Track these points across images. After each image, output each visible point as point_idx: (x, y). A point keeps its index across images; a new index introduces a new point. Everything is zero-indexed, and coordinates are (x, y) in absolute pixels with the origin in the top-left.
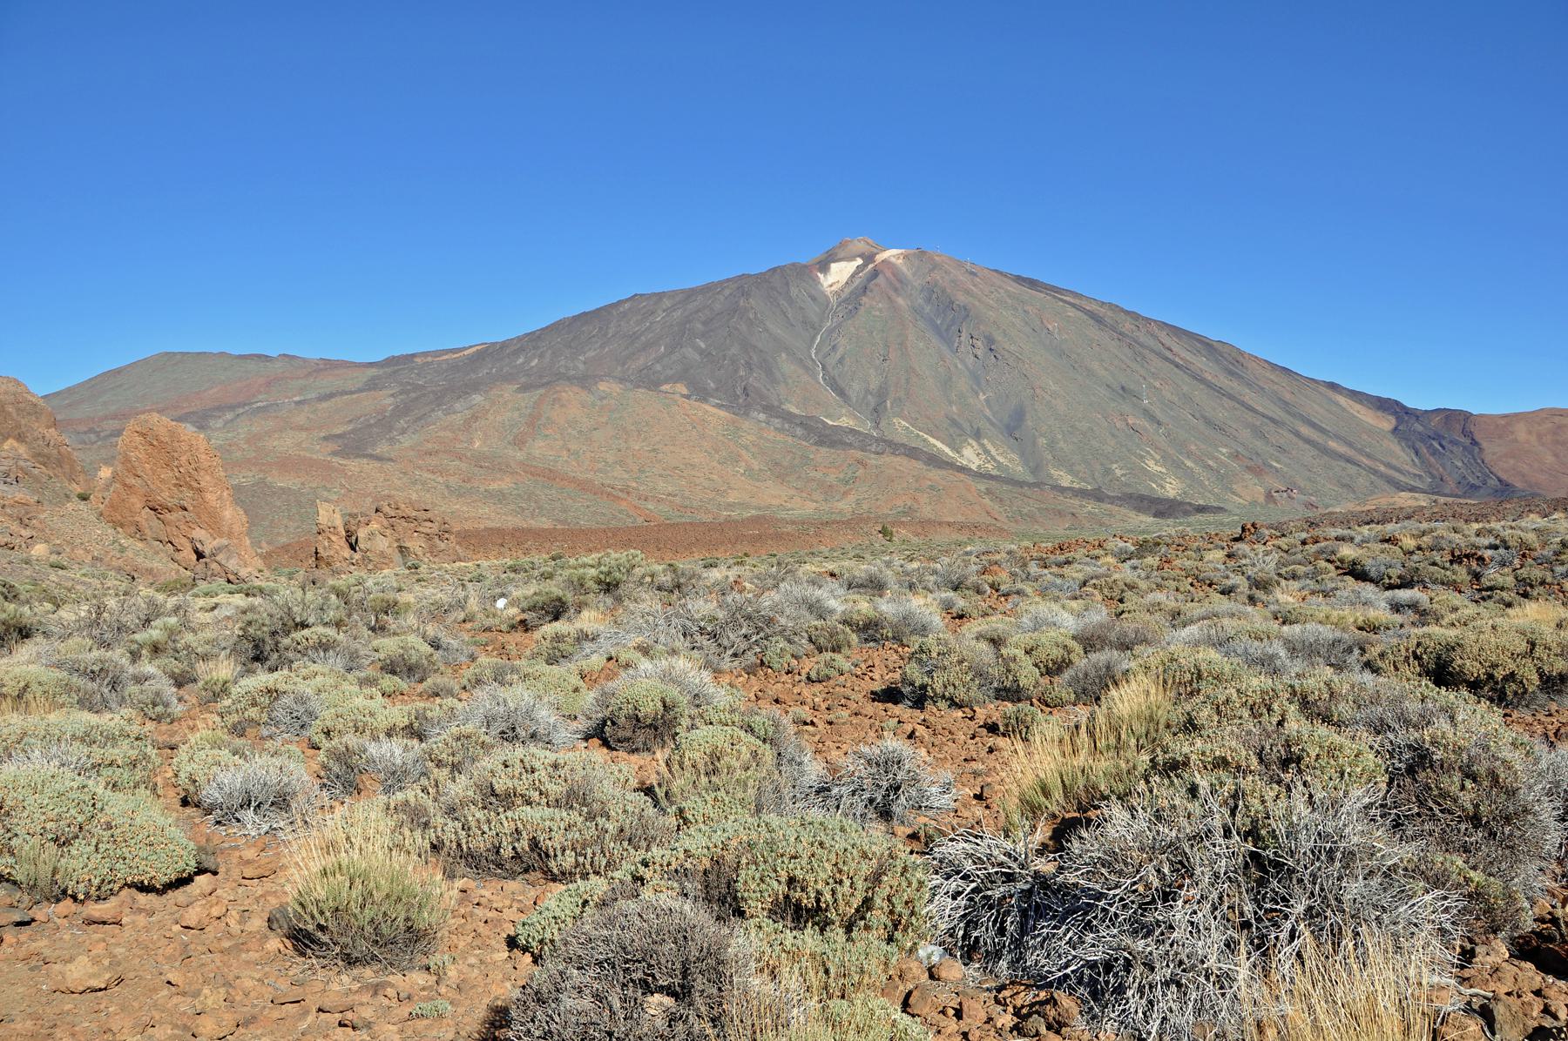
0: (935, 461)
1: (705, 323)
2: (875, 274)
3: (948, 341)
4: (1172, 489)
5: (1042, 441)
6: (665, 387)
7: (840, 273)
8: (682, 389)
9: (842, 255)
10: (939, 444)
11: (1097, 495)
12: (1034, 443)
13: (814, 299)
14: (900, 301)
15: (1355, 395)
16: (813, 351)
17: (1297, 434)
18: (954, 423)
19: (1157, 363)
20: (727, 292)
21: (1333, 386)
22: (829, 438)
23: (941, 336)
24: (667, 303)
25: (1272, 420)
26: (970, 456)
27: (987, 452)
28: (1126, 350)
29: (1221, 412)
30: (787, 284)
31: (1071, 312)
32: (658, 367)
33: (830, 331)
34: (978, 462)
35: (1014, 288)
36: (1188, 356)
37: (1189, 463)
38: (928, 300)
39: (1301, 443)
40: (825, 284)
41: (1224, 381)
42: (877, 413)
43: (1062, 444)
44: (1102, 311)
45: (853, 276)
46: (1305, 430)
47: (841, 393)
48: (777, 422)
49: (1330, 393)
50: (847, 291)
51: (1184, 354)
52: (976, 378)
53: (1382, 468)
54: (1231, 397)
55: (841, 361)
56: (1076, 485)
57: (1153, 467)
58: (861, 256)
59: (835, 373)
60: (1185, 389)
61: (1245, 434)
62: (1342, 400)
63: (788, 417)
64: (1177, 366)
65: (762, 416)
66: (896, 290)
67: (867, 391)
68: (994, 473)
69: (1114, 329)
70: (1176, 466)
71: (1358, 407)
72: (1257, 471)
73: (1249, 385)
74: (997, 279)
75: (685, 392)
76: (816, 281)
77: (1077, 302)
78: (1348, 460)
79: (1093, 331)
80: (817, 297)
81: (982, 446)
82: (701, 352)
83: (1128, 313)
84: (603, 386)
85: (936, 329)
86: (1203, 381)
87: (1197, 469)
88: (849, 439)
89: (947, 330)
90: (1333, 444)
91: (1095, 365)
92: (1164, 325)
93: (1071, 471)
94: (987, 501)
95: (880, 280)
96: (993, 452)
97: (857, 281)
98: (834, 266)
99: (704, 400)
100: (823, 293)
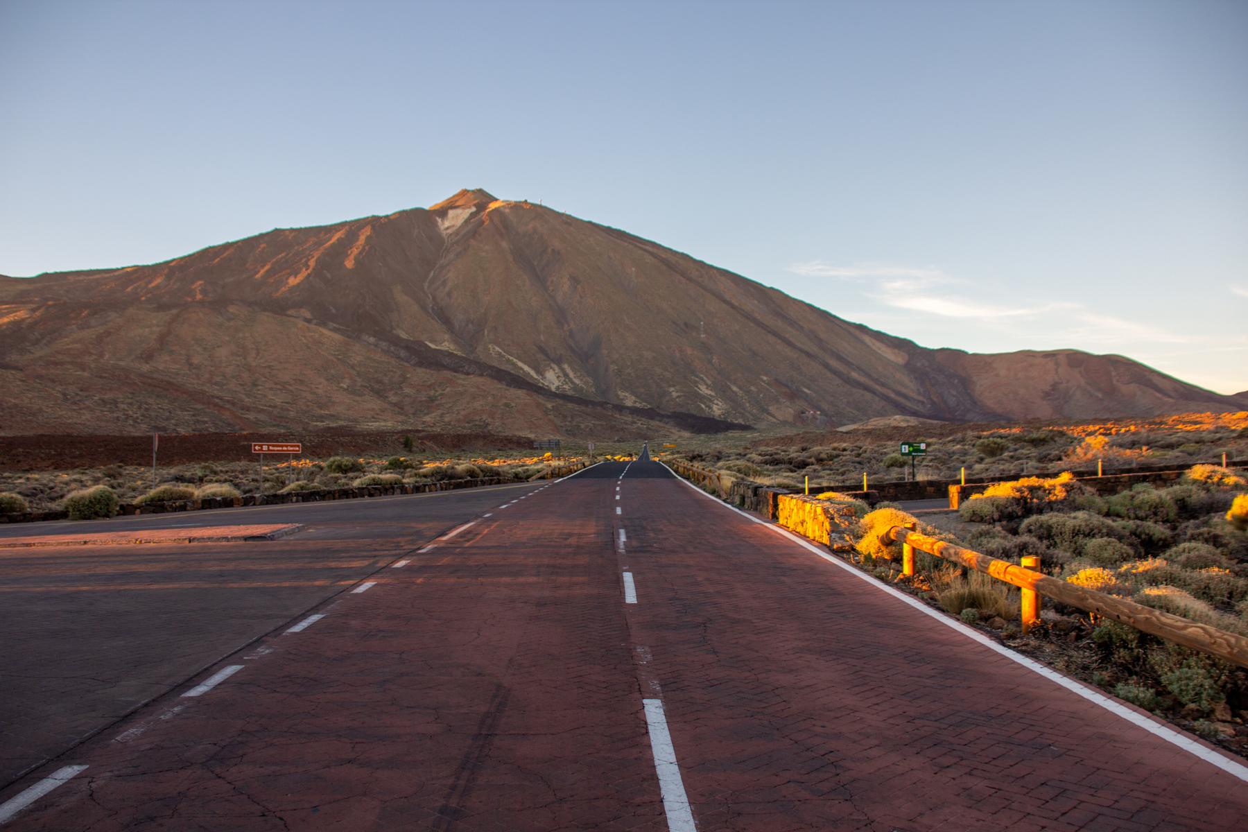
0: (518, 381)
4: (718, 409)
5: (613, 367)
6: (289, 312)
10: (526, 368)
11: (650, 414)
15: (879, 336)
16: (426, 285)
17: (827, 366)
18: (542, 350)
21: (861, 328)
22: (431, 360)
25: (808, 355)
26: (552, 379)
27: (566, 375)
31: (649, 259)
34: (557, 383)
37: (735, 389)
39: (829, 374)
40: (442, 228)
45: (467, 221)
46: (833, 363)
48: (384, 345)
49: (858, 333)
53: (892, 395)
54: (775, 334)
55: (449, 294)
56: (638, 405)
57: (704, 390)
62: (867, 339)
63: (396, 342)
64: (733, 307)
65: (372, 340)
68: (570, 393)
70: (722, 391)
71: (878, 344)
72: (793, 395)
75: (308, 315)
76: (435, 225)
77: (655, 251)
78: (867, 388)
80: (435, 238)
81: (563, 370)
84: (232, 309)
87: (740, 393)
88: (446, 361)
90: (854, 375)
93: (634, 393)
94: (552, 417)
96: (571, 375)
97: (470, 226)
98: (451, 213)
99: (323, 324)
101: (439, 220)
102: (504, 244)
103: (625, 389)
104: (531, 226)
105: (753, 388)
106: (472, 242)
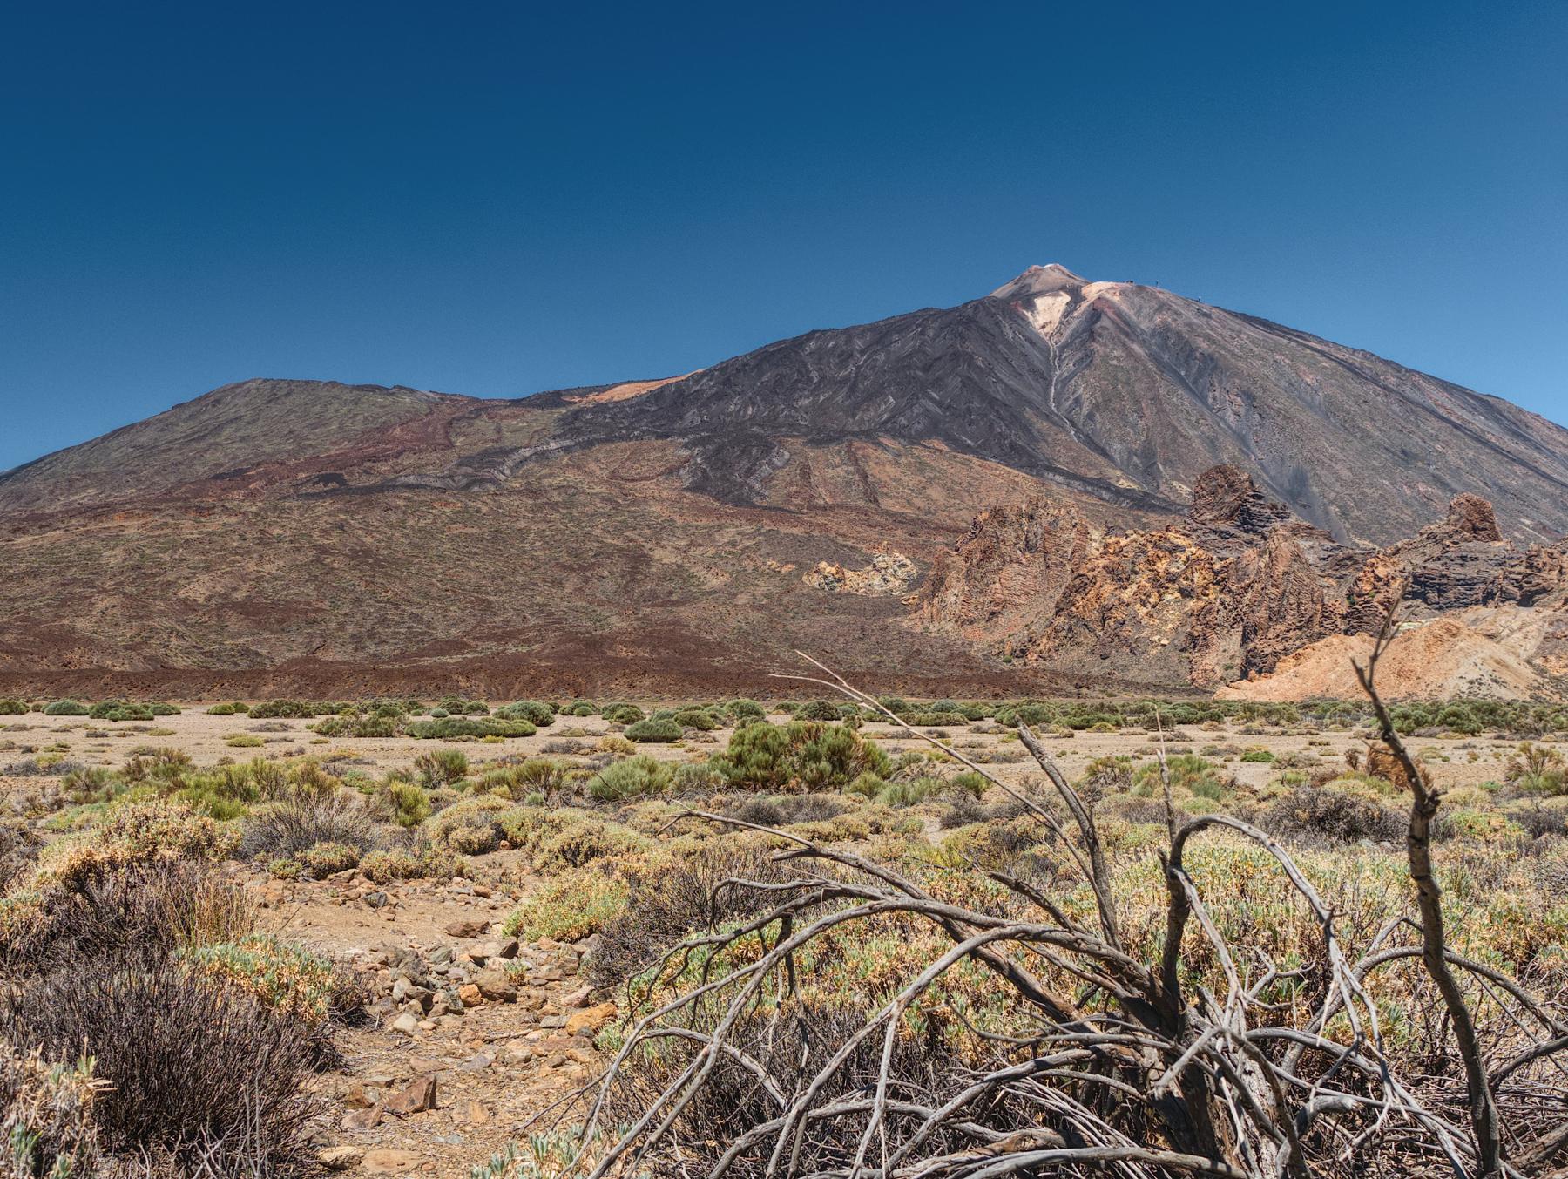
1: (927, 369)
2: (1095, 314)
3: (1203, 399)
5: (1333, 509)
7: (1048, 312)
8: (936, 443)
9: (1036, 287)
12: (1327, 513)
13: (1032, 343)
14: (1136, 348)
16: (1053, 406)
19: (1436, 424)
20: (931, 333)
23: (1191, 390)
24: (859, 344)
28: (1396, 407)
29: (1516, 478)
30: (997, 324)
32: (904, 421)
33: (1065, 382)
35: (1251, 332)
36: (1466, 415)
38: (1164, 347)
40: (1037, 325)
41: (1509, 443)
42: (1149, 472)
43: (1356, 513)
44: (1357, 360)
45: (1066, 314)
47: (1104, 453)
50: (1067, 333)
51: (1461, 412)
52: (1241, 439)
54: (1522, 463)
55: (1090, 416)
58: (1063, 288)
59: (1088, 429)
60: (1471, 454)
61: (1545, 504)
64: (1456, 426)
66: (1127, 335)
67: (1131, 452)
69: (1375, 382)
73: (1538, 448)
74: (1236, 324)
76: (1024, 319)
77: (1326, 349)
79: (1355, 386)
82: (939, 404)
83: (1387, 363)
85: (1182, 382)
86: (1486, 443)
89: (1195, 382)
91: (1368, 425)
92: (1430, 379)
95: (1104, 322)
98: (1039, 302)
100: (1037, 335)
101: (1029, 314)
102: (1136, 348)
103: (1361, 536)
104: (1158, 320)
105: (1517, 534)
106: (1096, 346)
